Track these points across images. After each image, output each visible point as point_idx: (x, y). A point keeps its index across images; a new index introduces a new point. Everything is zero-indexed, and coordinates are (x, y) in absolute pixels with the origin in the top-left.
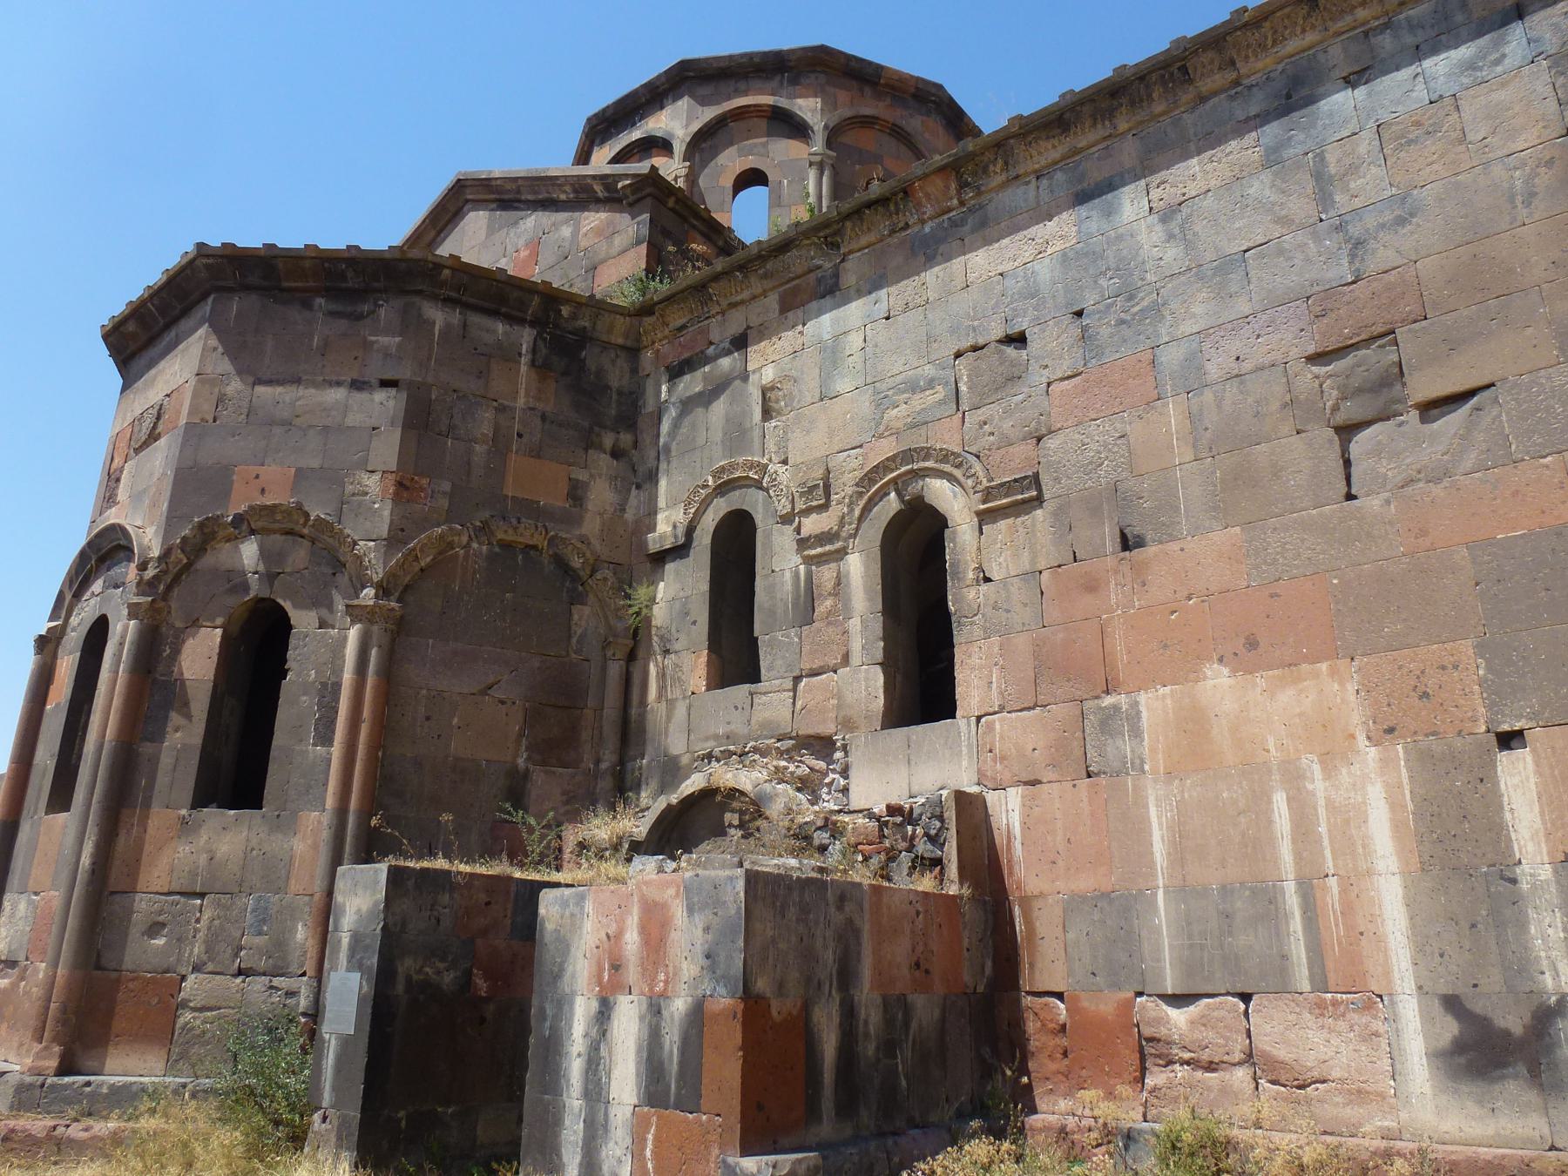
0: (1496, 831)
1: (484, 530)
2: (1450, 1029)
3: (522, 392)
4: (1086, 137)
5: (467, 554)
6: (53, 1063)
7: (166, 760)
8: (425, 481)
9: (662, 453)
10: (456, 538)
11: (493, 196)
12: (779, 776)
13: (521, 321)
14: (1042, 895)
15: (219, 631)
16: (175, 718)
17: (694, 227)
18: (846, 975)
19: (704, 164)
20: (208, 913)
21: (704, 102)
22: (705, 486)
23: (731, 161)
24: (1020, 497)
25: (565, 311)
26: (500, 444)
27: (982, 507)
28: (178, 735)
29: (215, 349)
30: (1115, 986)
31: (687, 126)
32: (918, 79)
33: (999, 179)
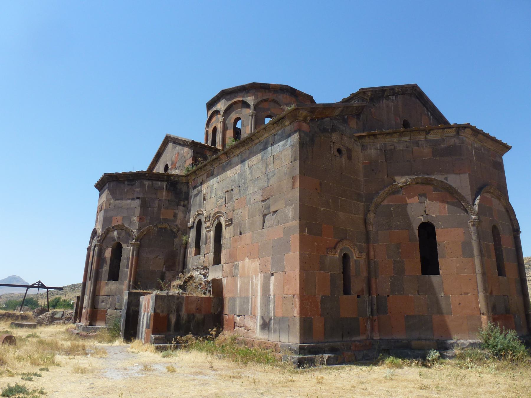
0: (269, 289)
1: (156, 225)
2: (262, 321)
4: (242, 149)
6: (88, 324)
7: (104, 272)
8: (145, 217)
9: (191, 206)
10: (151, 228)
11: (172, 140)
12: (201, 273)
14: (227, 297)
15: (111, 248)
16: (105, 265)
17: (206, 149)
18: (178, 310)
19: (228, 117)
20: (110, 299)
21: (228, 100)
22: (196, 214)
23: (233, 116)
24: (229, 223)
25: (172, 178)
26: (159, 208)
27: (226, 224)
28: (105, 268)
29: (109, 194)
30: (232, 313)
31: (224, 107)
32: (280, 85)
33: (232, 156)
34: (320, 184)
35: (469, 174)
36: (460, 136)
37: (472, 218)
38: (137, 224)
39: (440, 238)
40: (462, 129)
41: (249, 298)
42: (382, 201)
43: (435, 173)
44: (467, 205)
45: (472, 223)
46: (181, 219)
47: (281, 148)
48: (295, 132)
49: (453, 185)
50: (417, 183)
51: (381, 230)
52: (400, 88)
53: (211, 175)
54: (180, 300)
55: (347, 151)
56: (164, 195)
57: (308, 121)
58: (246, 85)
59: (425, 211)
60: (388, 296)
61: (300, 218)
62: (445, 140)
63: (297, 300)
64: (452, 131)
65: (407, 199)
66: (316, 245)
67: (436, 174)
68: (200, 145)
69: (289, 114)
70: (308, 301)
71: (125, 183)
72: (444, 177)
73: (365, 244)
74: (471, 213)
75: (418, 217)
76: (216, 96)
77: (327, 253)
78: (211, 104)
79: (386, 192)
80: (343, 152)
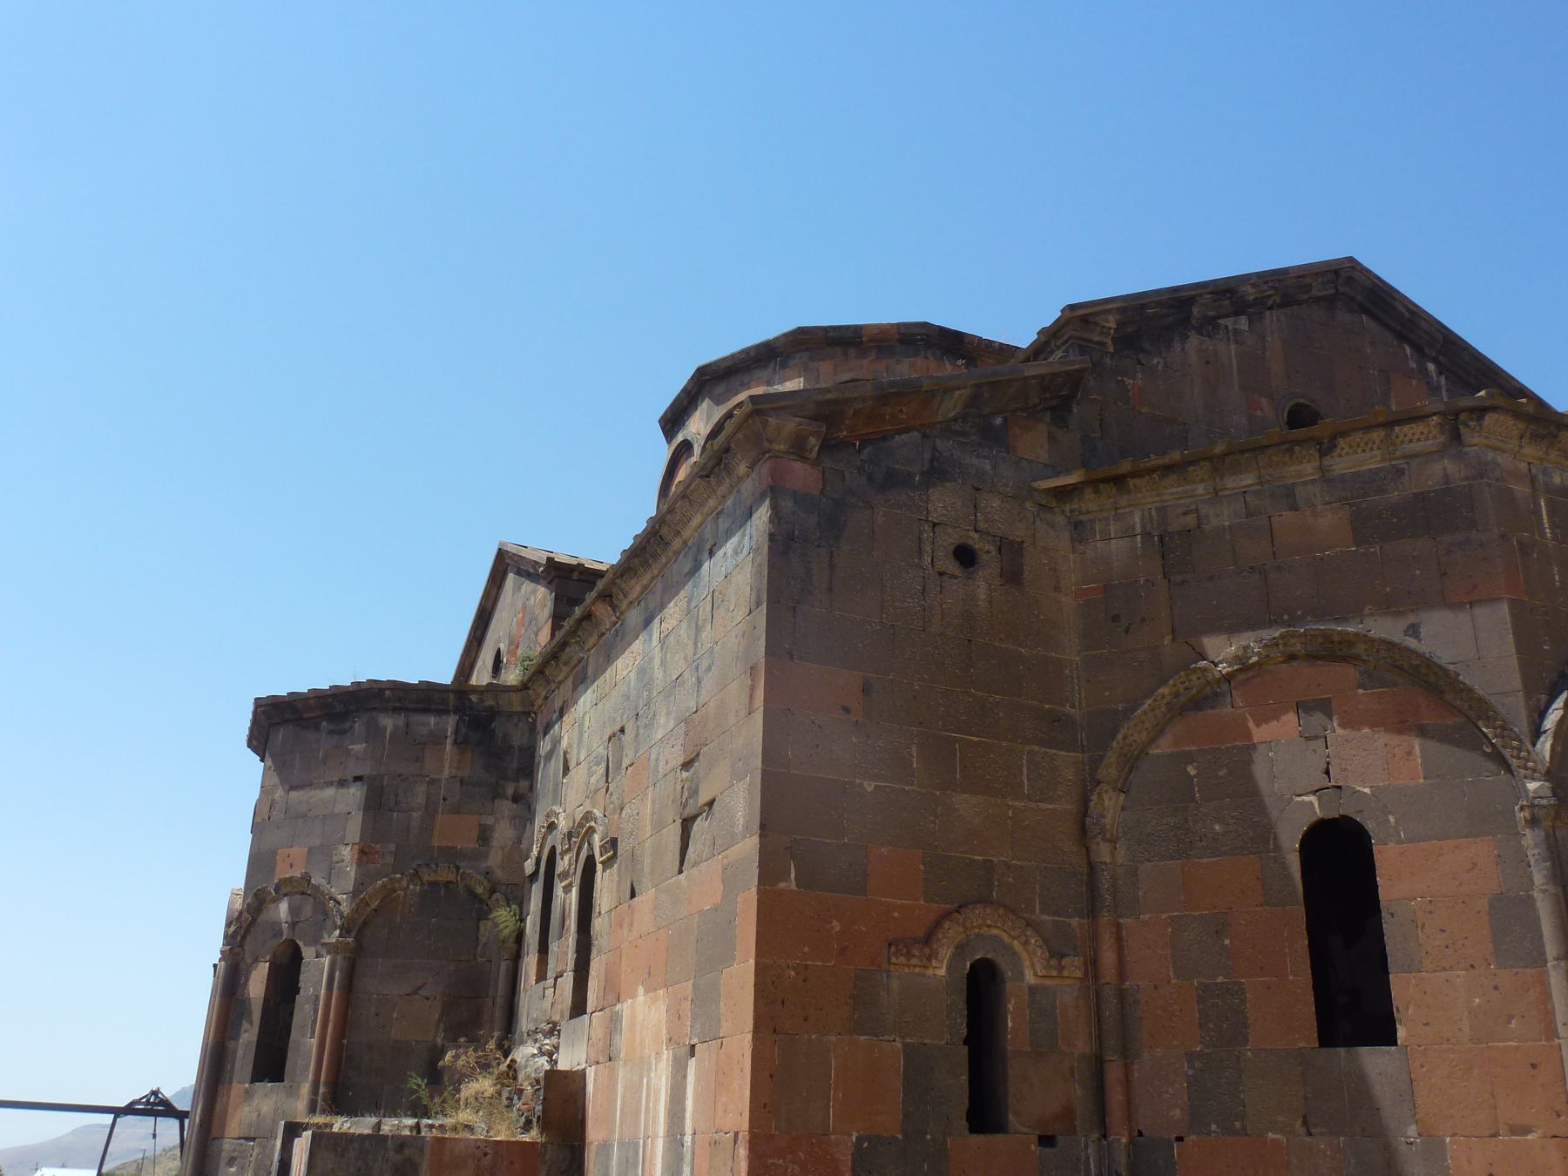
0: (683, 1110)
3: (447, 766)
5: (405, 894)
7: (240, 1052)
8: (378, 846)
10: (397, 885)
13: (447, 712)
15: (268, 963)
16: (245, 1025)
21: (718, 401)
22: (544, 827)
25: (474, 698)
26: (430, 810)
28: (247, 1034)
31: (705, 427)
32: (898, 325)
34: (866, 689)
35: (1513, 604)
36: (1466, 449)
37: (1526, 790)
38: (351, 870)
39: (1393, 885)
40: (1472, 419)
41: (639, 1143)
42: (1152, 741)
43: (1367, 611)
44: (1503, 737)
45: (1527, 814)
46: (502, 848)
47: (730, 563)
48: (762, 497)
49: (1444, 656)
50: (1292, 657)
51: (1149, 861)
52: (1266, 282)
53: (582, 680)
54: (407, 1152)
55: (1000, 551)
56: (447, 763)
57: (811, 450)
58: (777, 339)
59: (1327, 772)
60: (1179, 1139)
61: (762, 827)
62: (1404, 469)
63: (743, 1152)
64: (1429, 432)
65: (1251, 724)
66: (838, 929)
67: (1372, 614)
68: (581, 573)
69: (740, 436)
70: (789, 1157)
71: (322, 728)
72: (1403, 623)
73: (1085, 921)
74: (1523, 772)
75: (1300, 799)
76: (684, 390)
77: (890, 963)
78: (673, 421)
79: (1165, 701)
80: (985, 557)
